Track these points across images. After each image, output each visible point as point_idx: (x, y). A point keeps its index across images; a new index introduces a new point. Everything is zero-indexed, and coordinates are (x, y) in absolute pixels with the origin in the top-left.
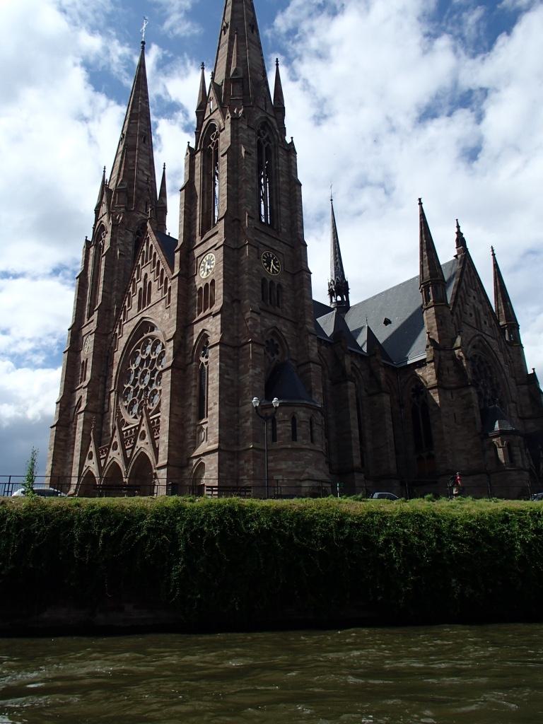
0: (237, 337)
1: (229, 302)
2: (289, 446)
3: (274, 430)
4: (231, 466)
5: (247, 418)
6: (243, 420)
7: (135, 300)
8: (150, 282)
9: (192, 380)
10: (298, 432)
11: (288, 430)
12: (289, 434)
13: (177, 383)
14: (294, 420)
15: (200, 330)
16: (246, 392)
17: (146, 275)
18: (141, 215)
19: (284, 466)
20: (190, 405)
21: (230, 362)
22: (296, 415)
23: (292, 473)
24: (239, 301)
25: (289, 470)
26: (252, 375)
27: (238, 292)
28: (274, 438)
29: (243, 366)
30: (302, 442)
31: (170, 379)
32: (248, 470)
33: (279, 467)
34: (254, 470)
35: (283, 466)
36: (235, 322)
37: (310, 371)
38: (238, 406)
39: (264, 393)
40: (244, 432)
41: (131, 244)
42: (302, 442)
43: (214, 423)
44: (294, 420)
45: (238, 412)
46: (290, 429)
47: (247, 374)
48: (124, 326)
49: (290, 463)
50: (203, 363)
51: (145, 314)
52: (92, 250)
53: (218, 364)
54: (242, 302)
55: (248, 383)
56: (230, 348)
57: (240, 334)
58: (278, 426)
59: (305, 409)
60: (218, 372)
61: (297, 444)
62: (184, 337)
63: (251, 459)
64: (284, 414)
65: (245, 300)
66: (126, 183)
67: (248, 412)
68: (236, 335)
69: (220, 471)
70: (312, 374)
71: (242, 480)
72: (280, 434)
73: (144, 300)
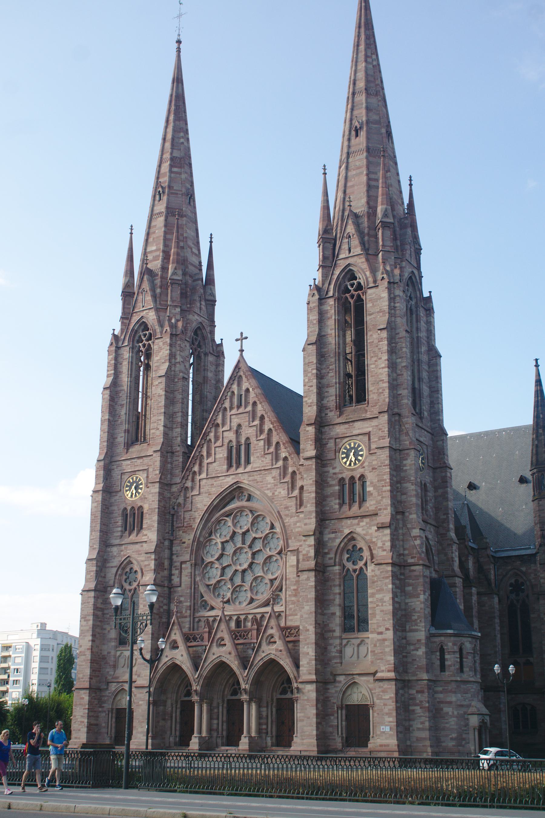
0: (403, 555)
1: (394, 513)
2: (459, 679)
3: (442, 660)
4: (403, 695)
5: (417, 646)
6: (412, 647)
7: (222, 454)
8: (248, 439)
9: (335, 586)
10: (464, 663)
11: (457, 662)
12: (458, 666)
13: (318, 588)
14: (461, 650)
15: (347, 531)
16: (416, 617)
17: (239, 426)
18: (196, 317)
19: (454, 699)
20: (334, 614)
21: (397, 582)
22: (463, 647)
23: (462, 706)
24: (403, 513)
25: (459, 703)
26: (420, 602)
27: (400, 502)
28: (443, 668)
29: (410, 588)
30: (468, 675)
31: (313, 584)
32: (421, 702)
33: (448, 699)
34: (428, 702)
35: (453, 698)
36: (401, 537)
37: (456, 587)
38: (404, 631)
39: (430, 618)
40: (413, 660)
42: (468, 675)
43: (387, 650)
44: (461, 650)
45: (405, 638)
46: (458, 660)
47: (418, 599)
48: (203, 482)
49: (459, 695)
50: (348, 569)
51: (241, 478)
52: (126, 354)
53: (390, 586)
54: (407, 514)
55: (418, 609)
56: (400, 568)
57: (406, 552)
58: (447, 656)
59: (470, 639)
60: (391, 595)
61: (465, 677)
62: (321, 533)
63: (426, 690)
64: (454, 644)
65: (411, 514)
66: (180, 272)
67: (419, 641)
68: (402, 552)
69: (397, 702)
70: (457, 590)
71: (414, 710)
72: (450, 666)
73: (238, 455)
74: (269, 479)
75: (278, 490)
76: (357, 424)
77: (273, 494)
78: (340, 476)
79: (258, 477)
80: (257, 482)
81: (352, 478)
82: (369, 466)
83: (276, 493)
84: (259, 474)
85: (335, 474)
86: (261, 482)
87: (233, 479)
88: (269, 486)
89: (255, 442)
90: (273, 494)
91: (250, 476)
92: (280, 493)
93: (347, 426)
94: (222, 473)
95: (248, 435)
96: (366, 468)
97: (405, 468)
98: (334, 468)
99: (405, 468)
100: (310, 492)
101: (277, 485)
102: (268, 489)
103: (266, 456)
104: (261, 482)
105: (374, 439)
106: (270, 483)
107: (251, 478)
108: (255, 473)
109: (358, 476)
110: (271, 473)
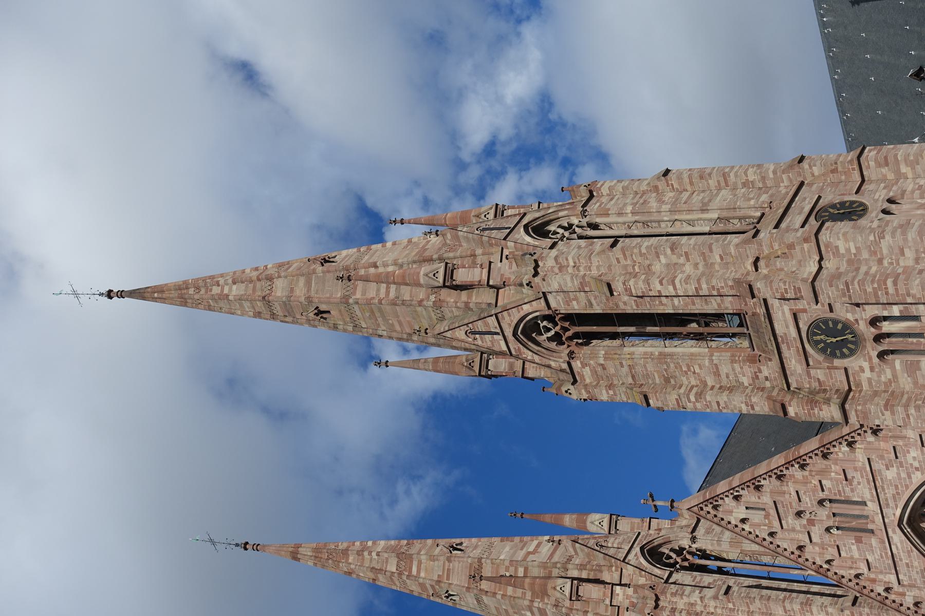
41: (698, 579)
74: (891, 474)
75: (911, 461)
76: (779, 330)
77: (917, 469)
78: (876, 360)
79: (889, 492)
80: (898, 494)
81: (878, 338)
82: (853, 313)
83: (916, 464)
84: (883, 490)
85: (872, 369)
86: (896, 487)
87: (894, 532)
88: (903, 475)
89: (826, 492)
90: (917, 469)
91: (888, 505)
92: (914, 458)
93: (784, 347)
94: (885, 549)
95: (815, 503)
96: (857, 316)
97: (853, 251)
98: (862, 370)
99: (853, 251)
100: (908, 416)
101: (901, 463)
102: (910, 477)
103: (849, 477)
104: (896, 487)
105: (800, 305)
106: (899, 474)
107: (892, 503)
108: (882, 496)
109: (872, 330)
110: (880, 471)
